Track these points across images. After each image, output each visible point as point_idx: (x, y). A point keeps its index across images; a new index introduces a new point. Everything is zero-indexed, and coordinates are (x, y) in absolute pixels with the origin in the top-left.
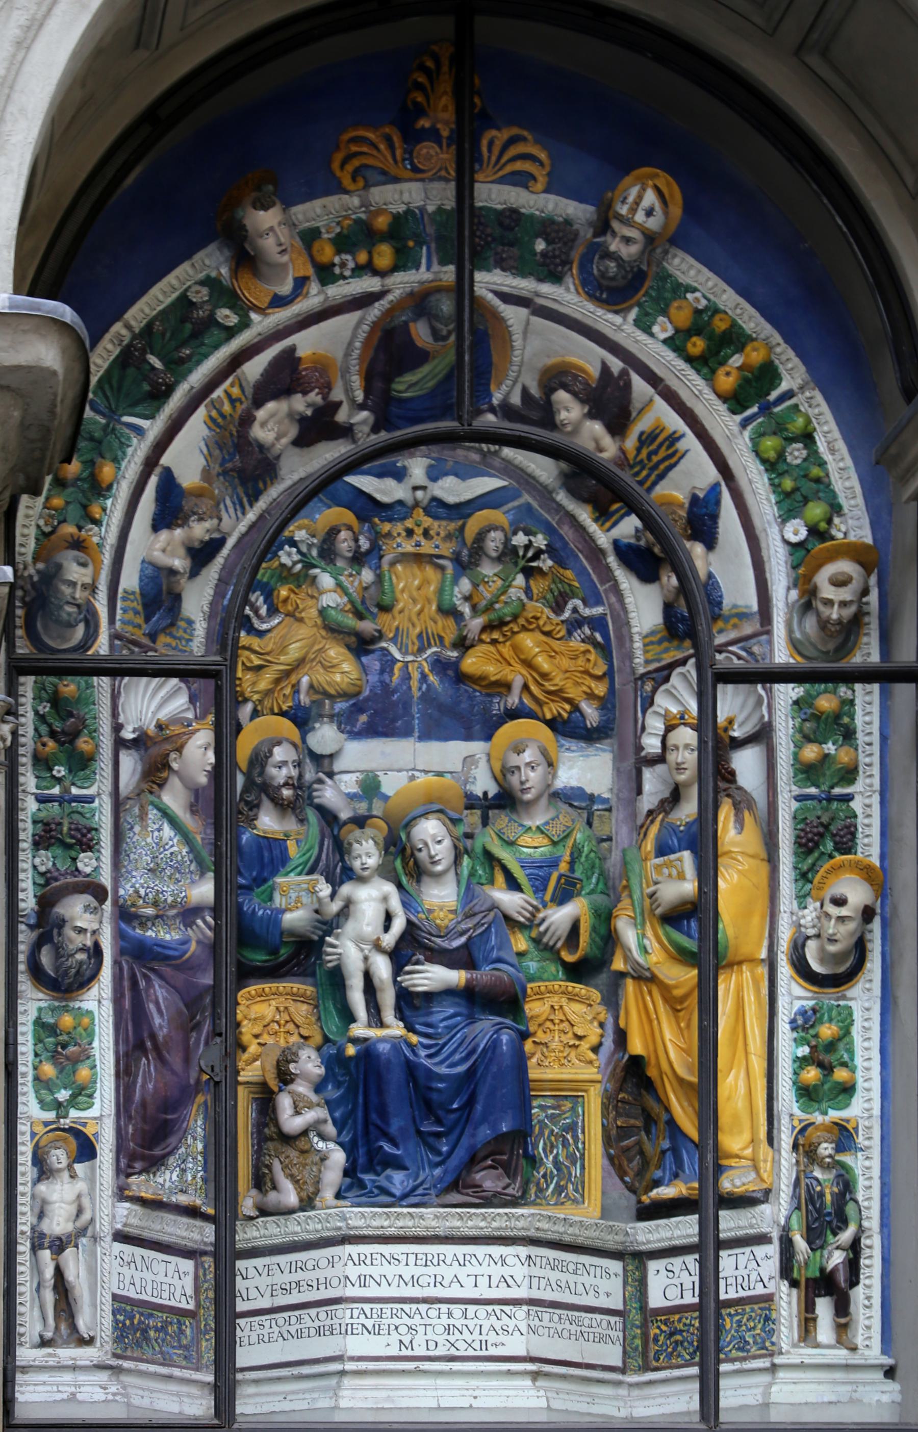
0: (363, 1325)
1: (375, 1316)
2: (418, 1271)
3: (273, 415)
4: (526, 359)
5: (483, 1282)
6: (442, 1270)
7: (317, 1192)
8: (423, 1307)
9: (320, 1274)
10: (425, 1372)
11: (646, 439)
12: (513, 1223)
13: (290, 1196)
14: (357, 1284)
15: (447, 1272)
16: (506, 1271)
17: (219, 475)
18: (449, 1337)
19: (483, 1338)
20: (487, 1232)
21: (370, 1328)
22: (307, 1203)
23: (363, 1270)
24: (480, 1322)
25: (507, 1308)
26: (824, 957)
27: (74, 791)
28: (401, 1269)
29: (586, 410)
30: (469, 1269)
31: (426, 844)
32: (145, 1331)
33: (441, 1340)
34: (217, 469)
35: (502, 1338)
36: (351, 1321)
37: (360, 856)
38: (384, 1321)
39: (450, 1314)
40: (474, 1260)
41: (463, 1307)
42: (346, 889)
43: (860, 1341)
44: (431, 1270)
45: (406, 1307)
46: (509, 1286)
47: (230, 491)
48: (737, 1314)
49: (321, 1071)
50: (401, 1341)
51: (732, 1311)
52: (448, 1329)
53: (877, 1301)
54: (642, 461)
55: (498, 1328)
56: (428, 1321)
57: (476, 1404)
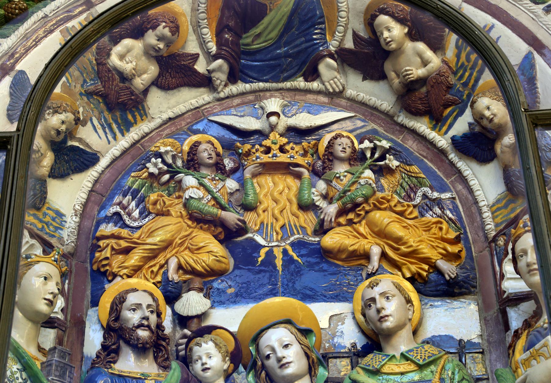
3: (129, 51)
4: (350, 6)
17: (81, 94)
29: (406, 30)
31: (273, 350)
37: (200, 358)
47: (96, 113)
54: (463, 64)
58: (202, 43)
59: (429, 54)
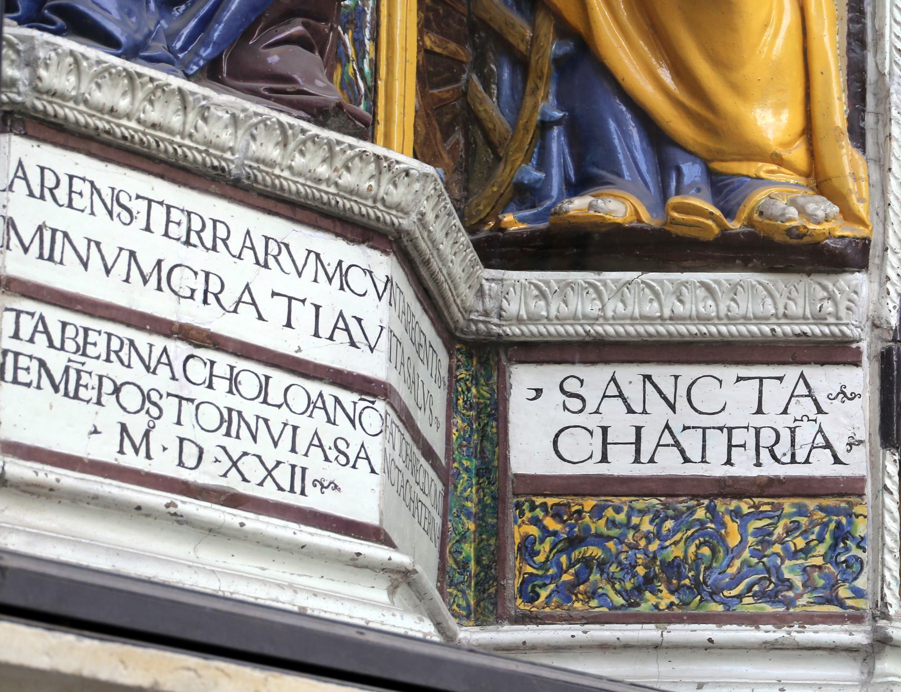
0: (42, 364)
1: (70, 346)
2: (173, 252)
6: (219, 262)
8: (179, 349)
10: (180, 520)
12: (385, 188)
14: (34, 249)
16: (351, 305)
18: (228, 442)
19: (299, 460)
20: (326, 193)
21: (58, 376)
23: (59, 218)
24: (294, 420)
25: (348, 398)
33: (210, 442)
35: (333, 472)
36: (14, 345)
38: (91, 365)
39: (233, 381)
40: (284, 258)
41: (262, 370)
44: (198, 258)
45: (142, 339)
46: (353, 344)
48: (758, 514)
50: (124, 428)
51: (745, 507)
55: (328, 443)
56: (187, 391)
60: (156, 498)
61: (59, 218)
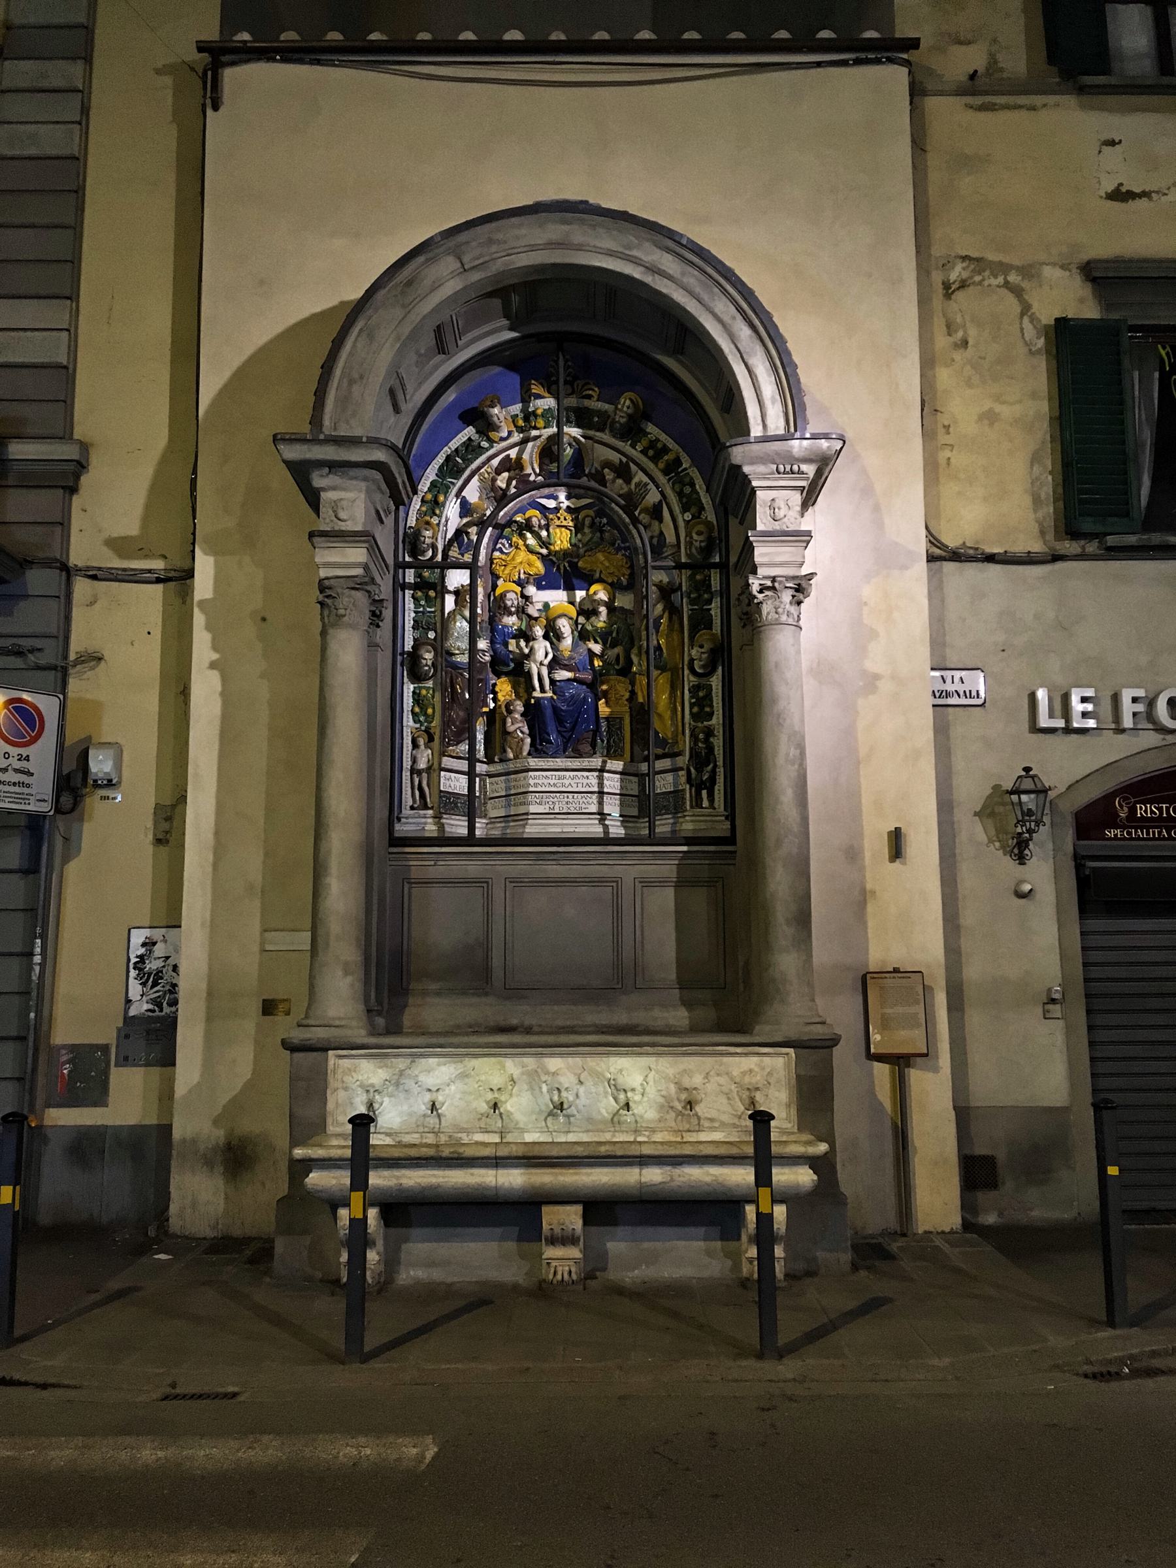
5: (580, 785)
6: (565, 781)
7: (521, 753)
8: (558, 795)
9: (522, 783)
11: (637, 485)
13: (511, 755)
15: (567, 782)
16: (589, 781)
22: (516, 757)
23: (536, 781)
26: (703, 667)
27: (428, 609)
28: (550, 781)
30: (575, 781)
32: (456, 804)
34: (485, 497)
42: (531, 644)
43: (716, 806)
44: (561, 781)
49: (523, 709)
52: (567, 803)
53: (722, 792)
57: (577, 830)
58: (533, 469)
59: (624, 486)
60: (552, 816)
61: (536, 781)
